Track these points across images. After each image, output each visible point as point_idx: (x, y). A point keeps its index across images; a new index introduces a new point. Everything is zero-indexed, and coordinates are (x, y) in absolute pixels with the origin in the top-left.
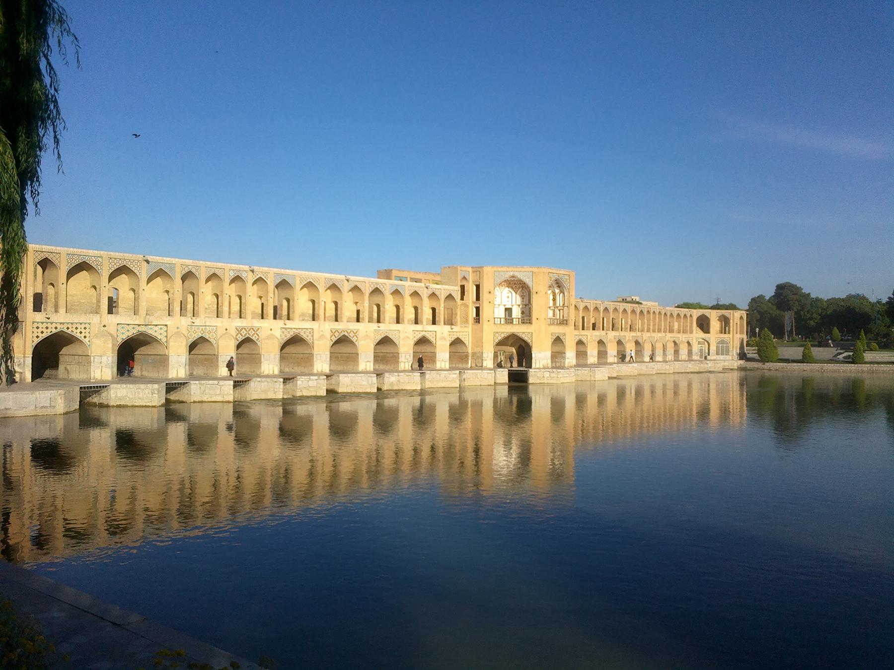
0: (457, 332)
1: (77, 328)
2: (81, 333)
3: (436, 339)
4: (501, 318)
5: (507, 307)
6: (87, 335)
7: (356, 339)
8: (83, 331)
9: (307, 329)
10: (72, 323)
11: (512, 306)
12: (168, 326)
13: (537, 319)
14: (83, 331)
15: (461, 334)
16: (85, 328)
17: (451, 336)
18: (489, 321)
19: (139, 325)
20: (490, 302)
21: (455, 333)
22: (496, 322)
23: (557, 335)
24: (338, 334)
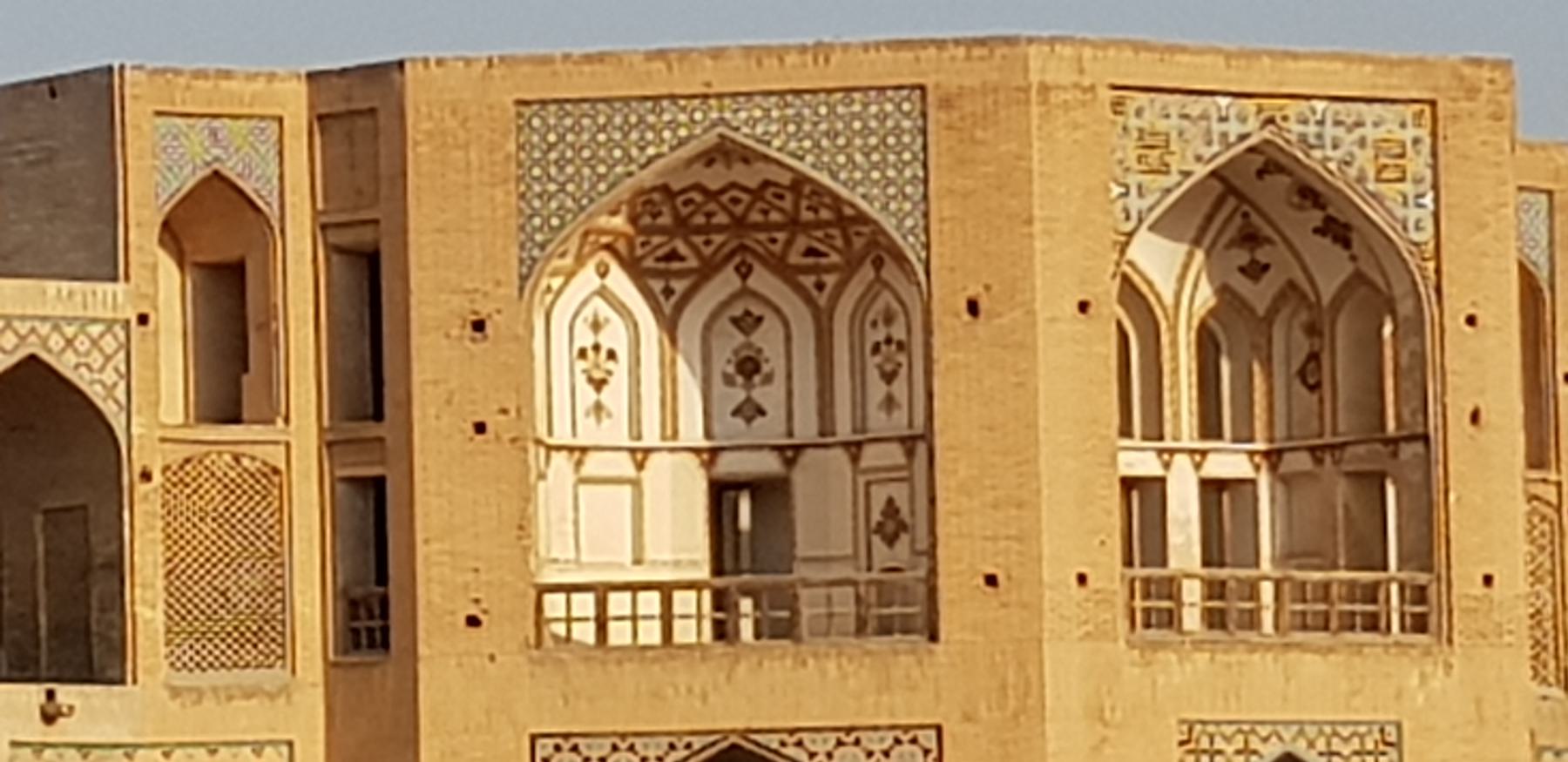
4: (666, 590)
5: (729, 465)
11: (791, 453)
20: (480, 428)
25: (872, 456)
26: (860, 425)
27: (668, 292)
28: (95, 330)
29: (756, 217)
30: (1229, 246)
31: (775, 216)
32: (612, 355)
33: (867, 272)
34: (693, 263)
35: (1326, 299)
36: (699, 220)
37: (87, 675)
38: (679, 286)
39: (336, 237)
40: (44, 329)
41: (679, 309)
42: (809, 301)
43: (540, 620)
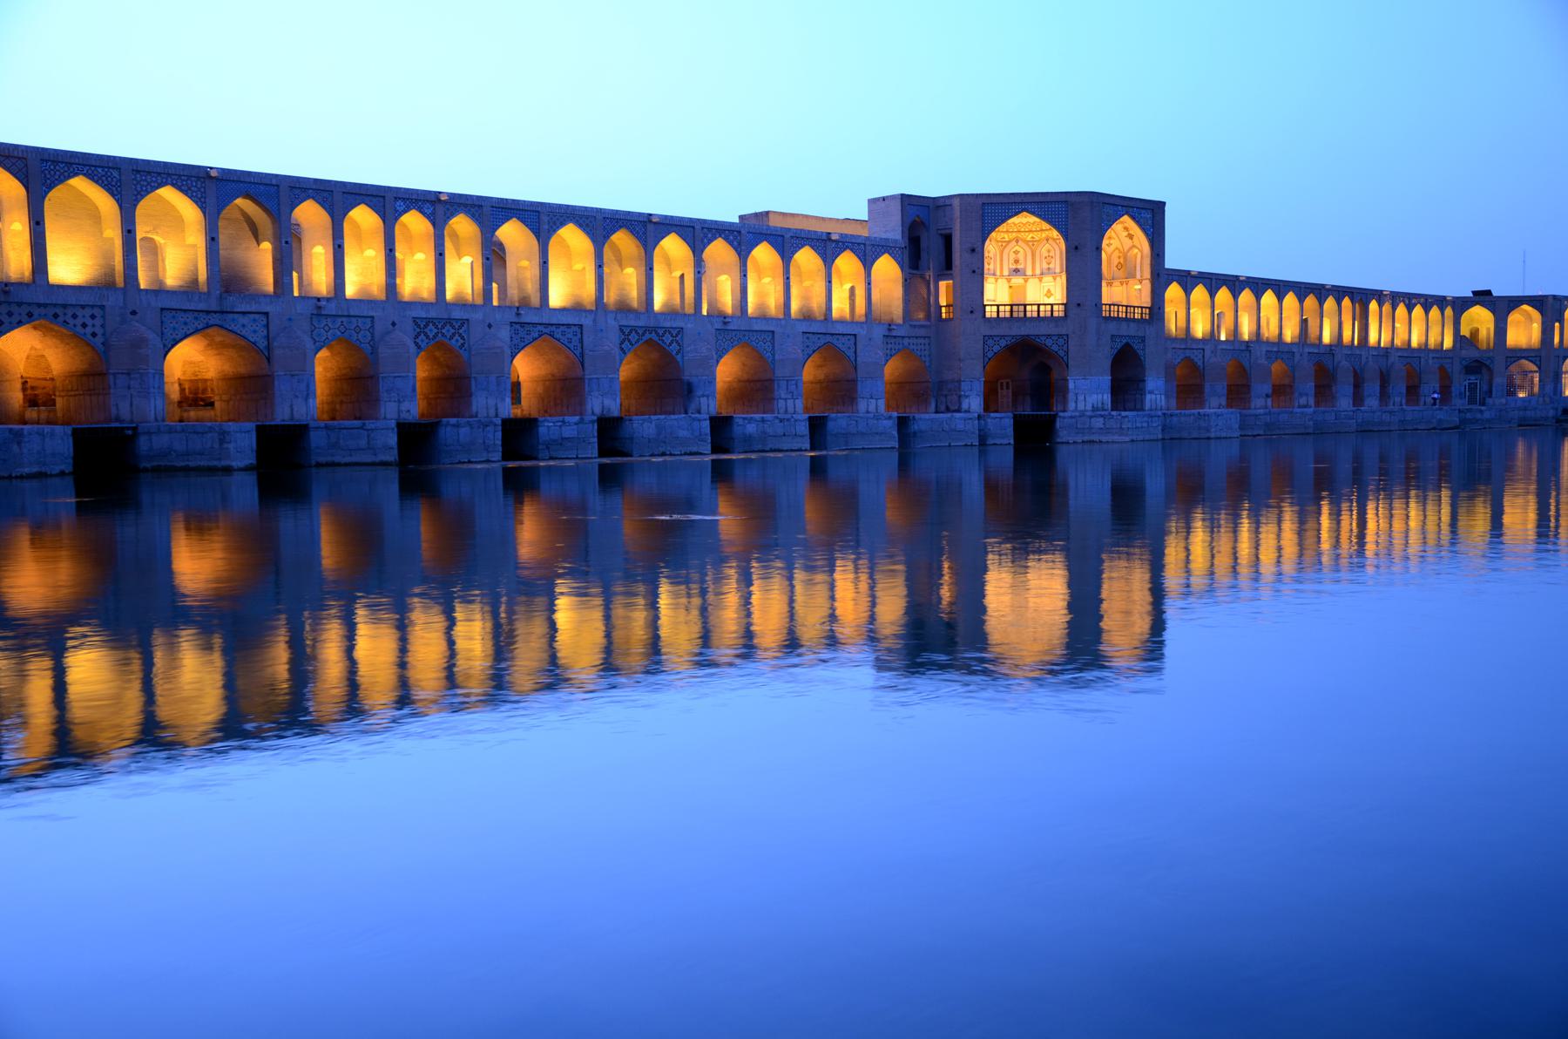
0: (903, 337)
1: (75, 316)
2: (84, 325)
3: (855, 352)
6: (99, 331)
8: (89, 322)
9: (568, 325)
10: (65, 306)
12: (270, 314)
13: (1079, 305)
14: (89, 322)
16: (93, 317)
17: (890, 346)
18: (972, 312)
19: (208, 312)
21: (898, 340)
22: (988, 315)
23: (1124, 341)
24: (637, 337)
34: (1007, 239)
38: (1004, 244)
39: (939, 232)
41: (1004, 249)
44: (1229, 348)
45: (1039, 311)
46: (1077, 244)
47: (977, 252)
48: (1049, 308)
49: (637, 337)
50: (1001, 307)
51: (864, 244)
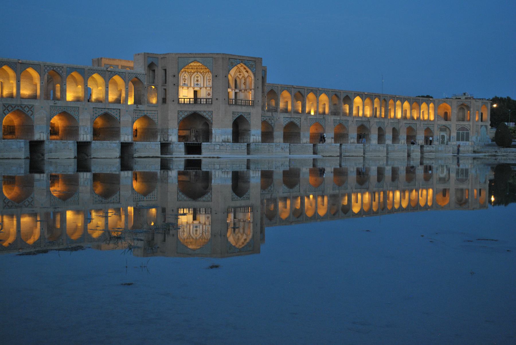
0: (144, 111)
7: (32, 113)
13: (217, 99)
15: (148, 112)
18: (173, 101)
24: (11, 108)
25: (208, 88)
26: (207, 86)
27: (191, 74)
28: (142, 75)
29: (198, 68)
30: (238, 73)
31: (200, 68)
32: (186, 79)
33: (208, 73)
34: (193, 72)
35: (246, 77)
36: (194, 68)
37: (141, 104)
38: (192, 74)
39: (162, 68)
40: (137, 75)
41: (192, 75)
42: (203, 75)
43: (179, 101)
44: (360, 120)
45: (184, 101)
46: (216, 75)
47: (176, 76)
48: (188, 100)
49: (11, 108)
50: (207, 100)
51: (125, 73)
